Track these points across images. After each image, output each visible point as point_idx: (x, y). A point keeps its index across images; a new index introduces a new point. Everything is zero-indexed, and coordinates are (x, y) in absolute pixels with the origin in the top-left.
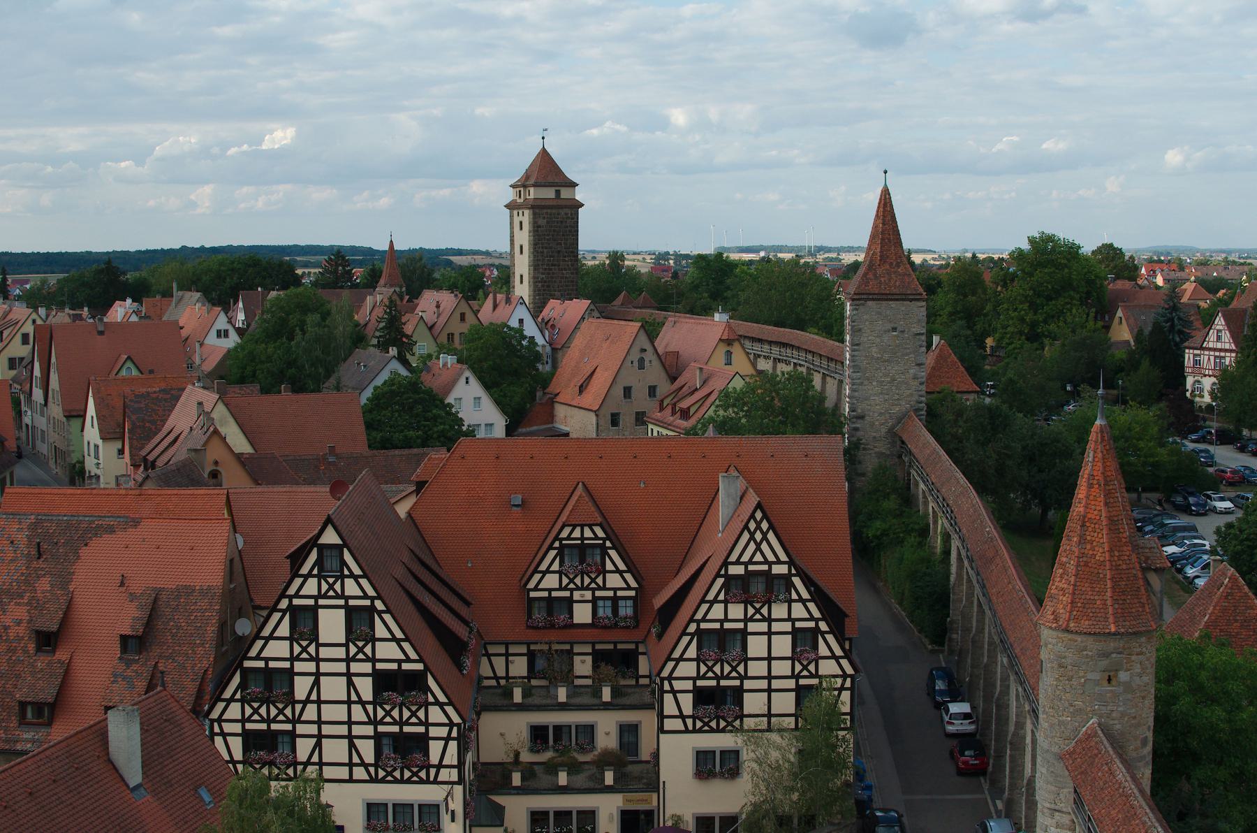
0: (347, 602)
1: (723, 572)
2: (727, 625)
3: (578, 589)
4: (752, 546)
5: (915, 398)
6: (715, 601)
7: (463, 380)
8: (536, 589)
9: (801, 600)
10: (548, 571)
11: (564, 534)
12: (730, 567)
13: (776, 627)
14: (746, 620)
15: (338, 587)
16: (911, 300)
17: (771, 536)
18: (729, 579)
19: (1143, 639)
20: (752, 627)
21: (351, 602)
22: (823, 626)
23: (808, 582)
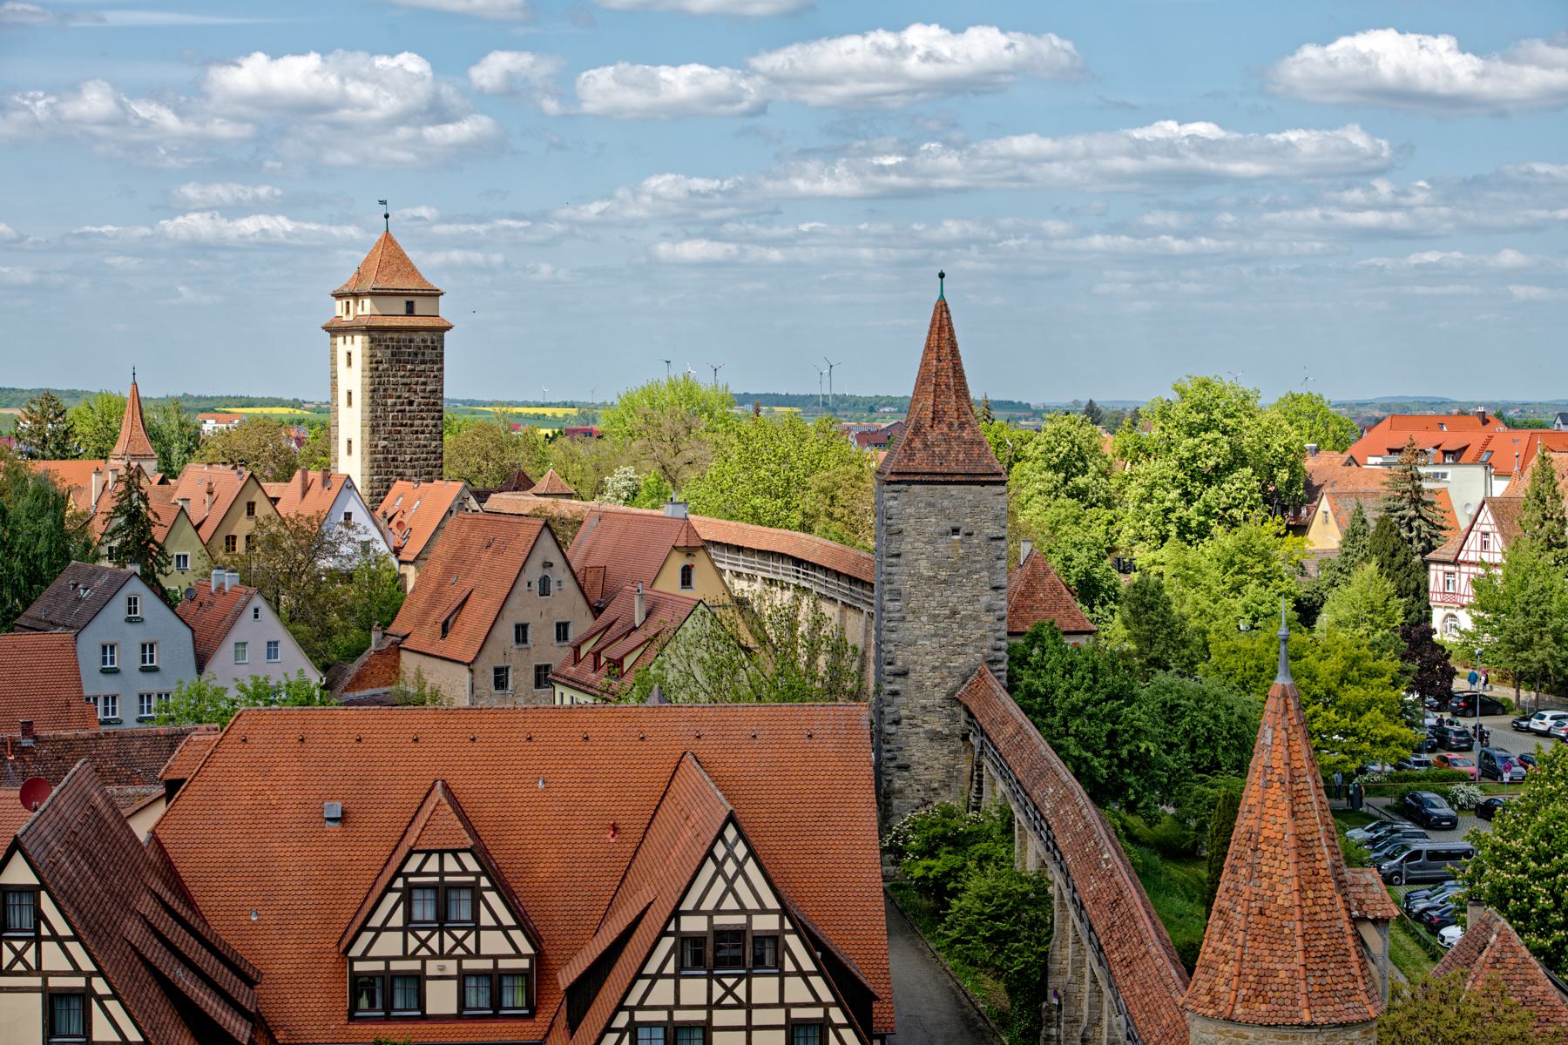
0: (45, 981)
1: (672, 928)
2: (679, 1016)
3: (434, 956)
4: (720, 885)
5: (991, 642)
6: (660, 974)
7: (250, 612)
8: (364, 957)
9: (800, 973)
10: (384, 928)
11: (412, 866)
12: (684, 919)
13: (759, 1017)
14: (710, 1006)
15: (30, 956)
16: (983, 484)
17: (751, 867)
18: (684, 939)
19: (1356, 1034)
20: (719, 1018)
21: (54, 982)
22: (837, 1016)
23: (813, 943)
